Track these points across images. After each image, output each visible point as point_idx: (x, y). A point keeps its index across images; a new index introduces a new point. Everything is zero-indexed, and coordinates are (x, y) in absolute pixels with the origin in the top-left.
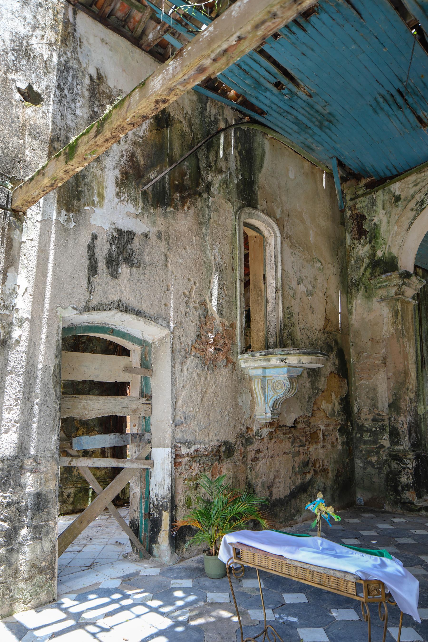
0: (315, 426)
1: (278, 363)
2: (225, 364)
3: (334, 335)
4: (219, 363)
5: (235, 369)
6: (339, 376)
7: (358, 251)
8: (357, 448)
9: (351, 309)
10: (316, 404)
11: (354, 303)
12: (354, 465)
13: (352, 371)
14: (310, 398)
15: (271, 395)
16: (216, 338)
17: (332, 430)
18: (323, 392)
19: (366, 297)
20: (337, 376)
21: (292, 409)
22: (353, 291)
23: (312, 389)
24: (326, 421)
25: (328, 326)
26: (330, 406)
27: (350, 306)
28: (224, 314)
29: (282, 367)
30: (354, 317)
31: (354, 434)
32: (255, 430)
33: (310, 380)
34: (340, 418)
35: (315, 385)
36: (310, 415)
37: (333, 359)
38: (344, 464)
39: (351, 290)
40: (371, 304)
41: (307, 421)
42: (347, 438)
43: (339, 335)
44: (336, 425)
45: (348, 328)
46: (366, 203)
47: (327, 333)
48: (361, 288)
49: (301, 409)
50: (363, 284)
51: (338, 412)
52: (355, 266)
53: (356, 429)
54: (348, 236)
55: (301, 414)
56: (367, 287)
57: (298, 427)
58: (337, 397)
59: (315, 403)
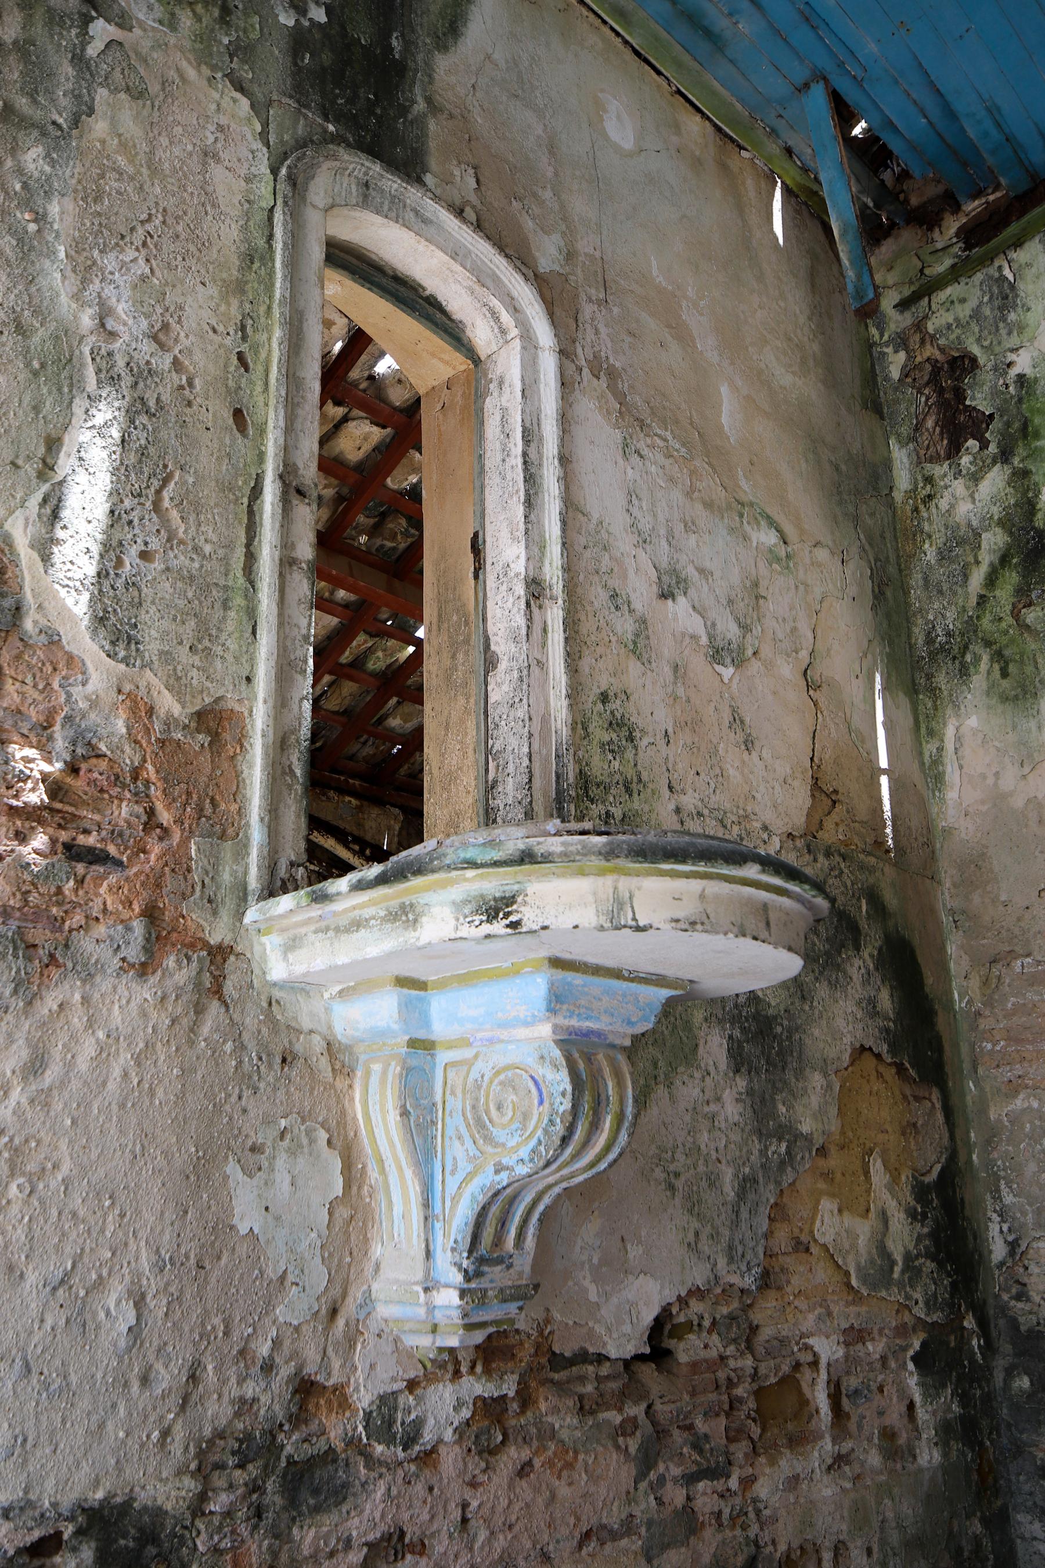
0: (783, 1342)
1: (465, 931)
2: (134, 953)
3: (862, 867)
4: (86, 944)
5: (217, 991)
6: (900, 1069)
7: (952, 506)
8: (1019, 1450)
9: (937, 761)
10: (786, 1218)
11: (950, 732)
12: (1012, 1551)
13: (964, 1049)
14: (746, 1185)
15: (464, 1167)
16: (78, 784)
17: (884, 1359)
18: (822, 1151)
19: (1004, 699)
20: (890, 1073)
21: (634, 1252)
22: (941, 680)
23: (760, 1133)
24: (846, 1314)
25: (829, 823)
26: (864, 1230)
27: (930, 748)
28: (152, 647)
29: (515, 971)
30: (952, 795)
31: (999, 1377)
32: (364, 1399)
33: (741, 1083)
34: (918, 1295)
35: (774, 1115)
36: (748, 1282)
37: (866, 982)
38: (960, 1550)
39: (929, 677)
40: (1033, 724)
41: (732, 1318)
42: (965, 1399)
43: (888, 869)
44: (902, 1331)
45: (928, 844)
46: (973, 303)
47: (828, 854)
48: (977, 659)
49: (693, 1247)
50: (988, 644)
51: (908, 1258)
52: (940, 574)
53: (1007, 1348)
54: (901, 457)
55: (699, 1276)
56: (1007, 652)
57: (683, 1358)
58: (895, 1179)
59: (778, 1213)
